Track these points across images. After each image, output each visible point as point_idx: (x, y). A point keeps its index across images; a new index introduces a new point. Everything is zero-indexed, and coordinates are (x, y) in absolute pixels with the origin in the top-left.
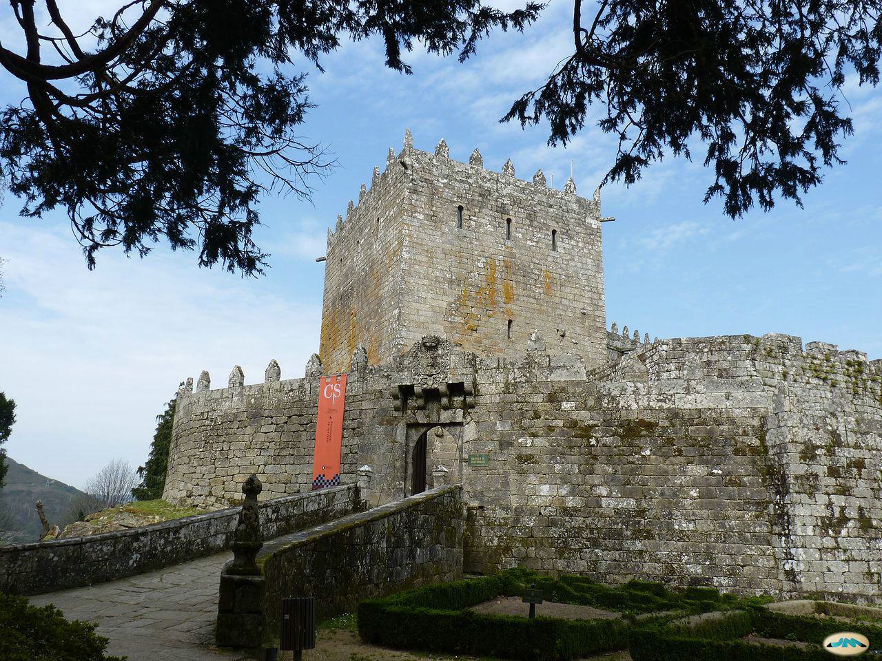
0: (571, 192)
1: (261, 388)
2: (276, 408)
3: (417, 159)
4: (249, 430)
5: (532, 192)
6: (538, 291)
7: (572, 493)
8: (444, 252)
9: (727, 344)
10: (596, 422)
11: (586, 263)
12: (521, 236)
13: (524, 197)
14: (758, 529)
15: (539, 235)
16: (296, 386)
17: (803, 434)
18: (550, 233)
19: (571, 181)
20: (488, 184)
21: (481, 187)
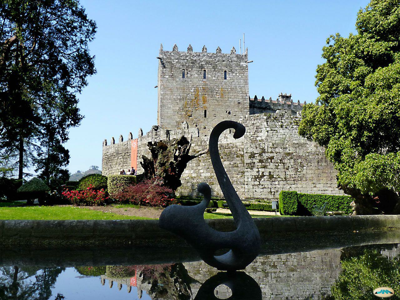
0: (233, 53)
2: (122, 151)
3: (165, 55)
4: (116, 158)
5: (215, 57)
6: (218, 97)
7: (194, 172)
8: (177, 88)
9: (259, 116)
10: (200, 150)
11: (240, 82)
12: (210, 76)
13: (211, 59)
14: (241, 180)
15: (218, 74)
16: (126, 143)
17: (250, 150)
18: (223, 72)
19: (234, 48)
20: (195, 58)
21: (192, 60)
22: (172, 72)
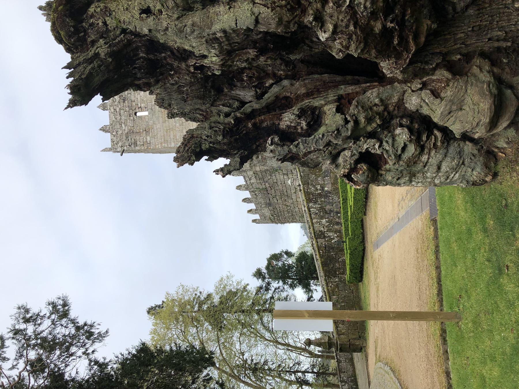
1: (255, 204)
21: (119, 102)
22: (141, 131)
